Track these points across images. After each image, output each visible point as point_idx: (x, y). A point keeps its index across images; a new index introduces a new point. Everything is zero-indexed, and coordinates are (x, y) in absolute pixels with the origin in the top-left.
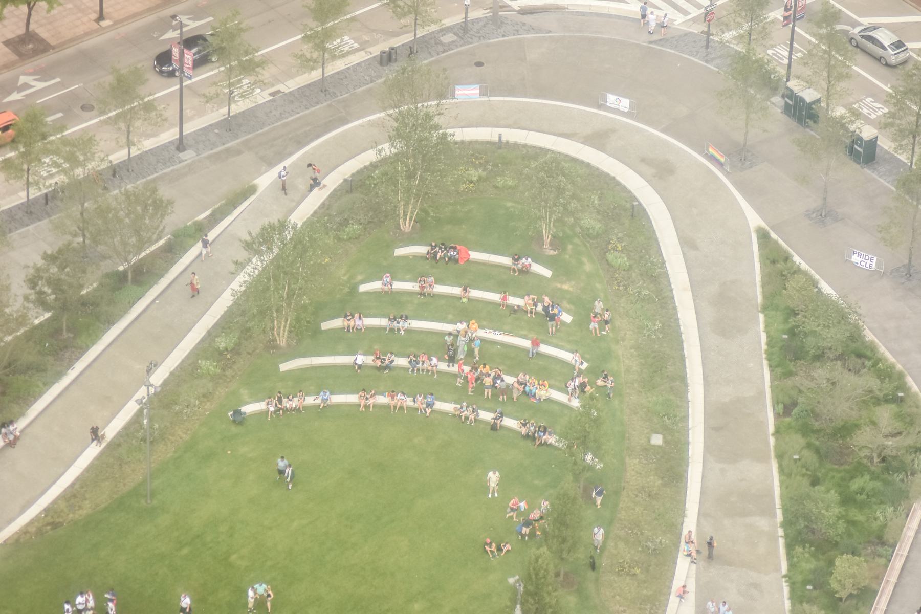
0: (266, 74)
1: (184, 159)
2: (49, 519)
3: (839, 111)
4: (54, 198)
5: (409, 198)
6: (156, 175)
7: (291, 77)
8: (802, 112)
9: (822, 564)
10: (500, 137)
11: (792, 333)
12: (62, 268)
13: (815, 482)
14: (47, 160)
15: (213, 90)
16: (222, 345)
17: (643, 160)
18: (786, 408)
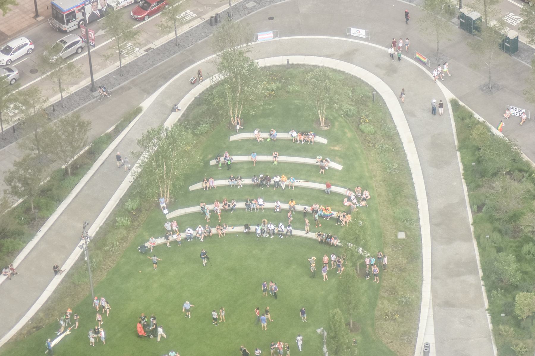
0: (141, 38)
1: (96, 96)
2: (35, 325)
3: (493, 23)
4: (18, 128)
5: (235, 104)
6: (80, 107)
7: (157, 39)
8: (469, 26)
9: (510, 300)
10: (288, 61)
11: (479, 162)
12: (26, 170)
13: (499, 250)
14: (12, 106)
15: (109, 52)
16: (130, 207)
17: (377, 66)
18: (478, 207)
